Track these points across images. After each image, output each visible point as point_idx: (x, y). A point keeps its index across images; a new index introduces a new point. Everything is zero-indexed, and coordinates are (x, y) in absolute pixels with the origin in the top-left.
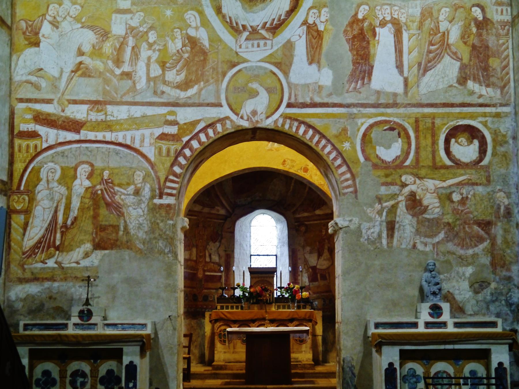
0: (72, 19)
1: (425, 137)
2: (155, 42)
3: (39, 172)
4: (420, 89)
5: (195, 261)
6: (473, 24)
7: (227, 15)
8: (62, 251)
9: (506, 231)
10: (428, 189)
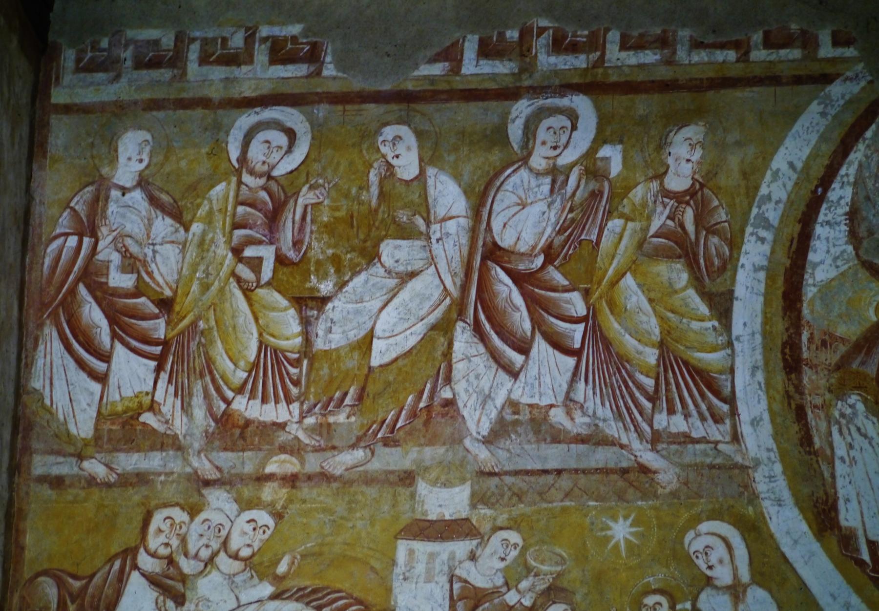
0: (237, 565)
7: (860, 533)
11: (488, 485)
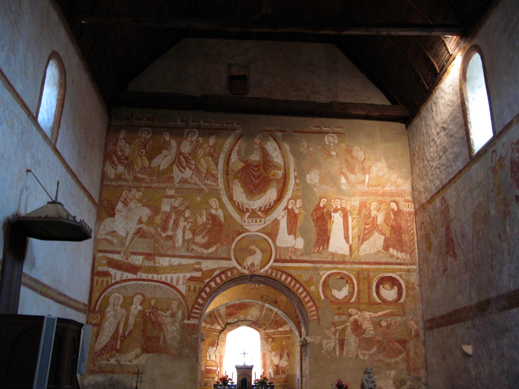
2: (189, 217)
4: (360, 253)
6: (391, 213)
8: (121, 353)
9: (415, 346)
10: (366, 318)
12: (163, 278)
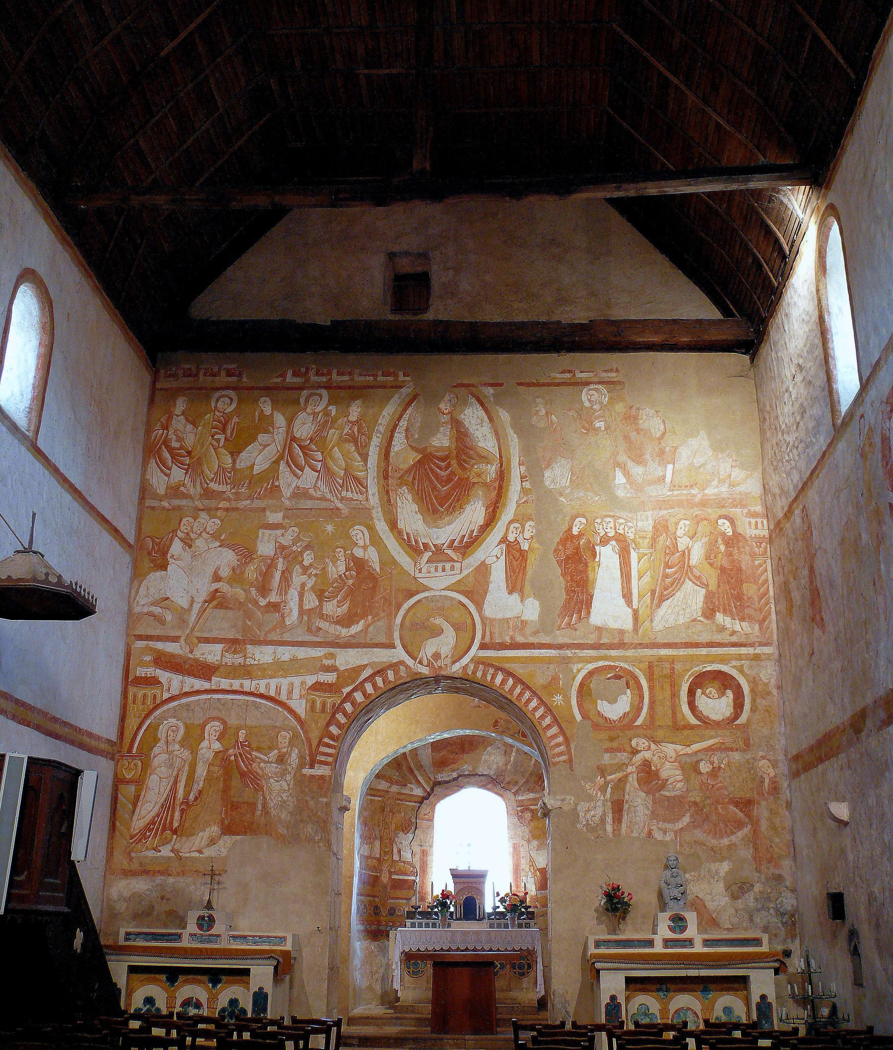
1: (662, 688)
3: (158, 729)
4: (654, 624)
5: (379, 860)
10: (667, 757)
11: (289, 513)
12: (261, 686)
